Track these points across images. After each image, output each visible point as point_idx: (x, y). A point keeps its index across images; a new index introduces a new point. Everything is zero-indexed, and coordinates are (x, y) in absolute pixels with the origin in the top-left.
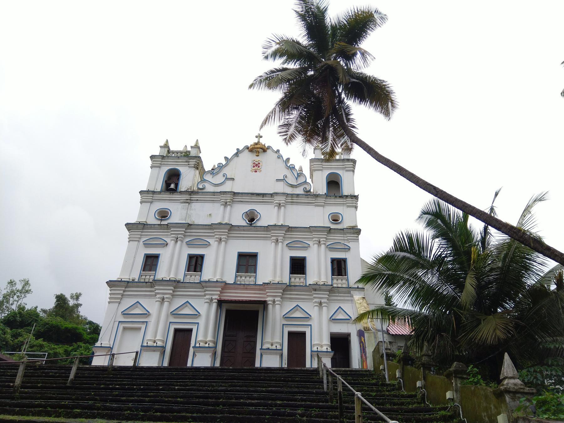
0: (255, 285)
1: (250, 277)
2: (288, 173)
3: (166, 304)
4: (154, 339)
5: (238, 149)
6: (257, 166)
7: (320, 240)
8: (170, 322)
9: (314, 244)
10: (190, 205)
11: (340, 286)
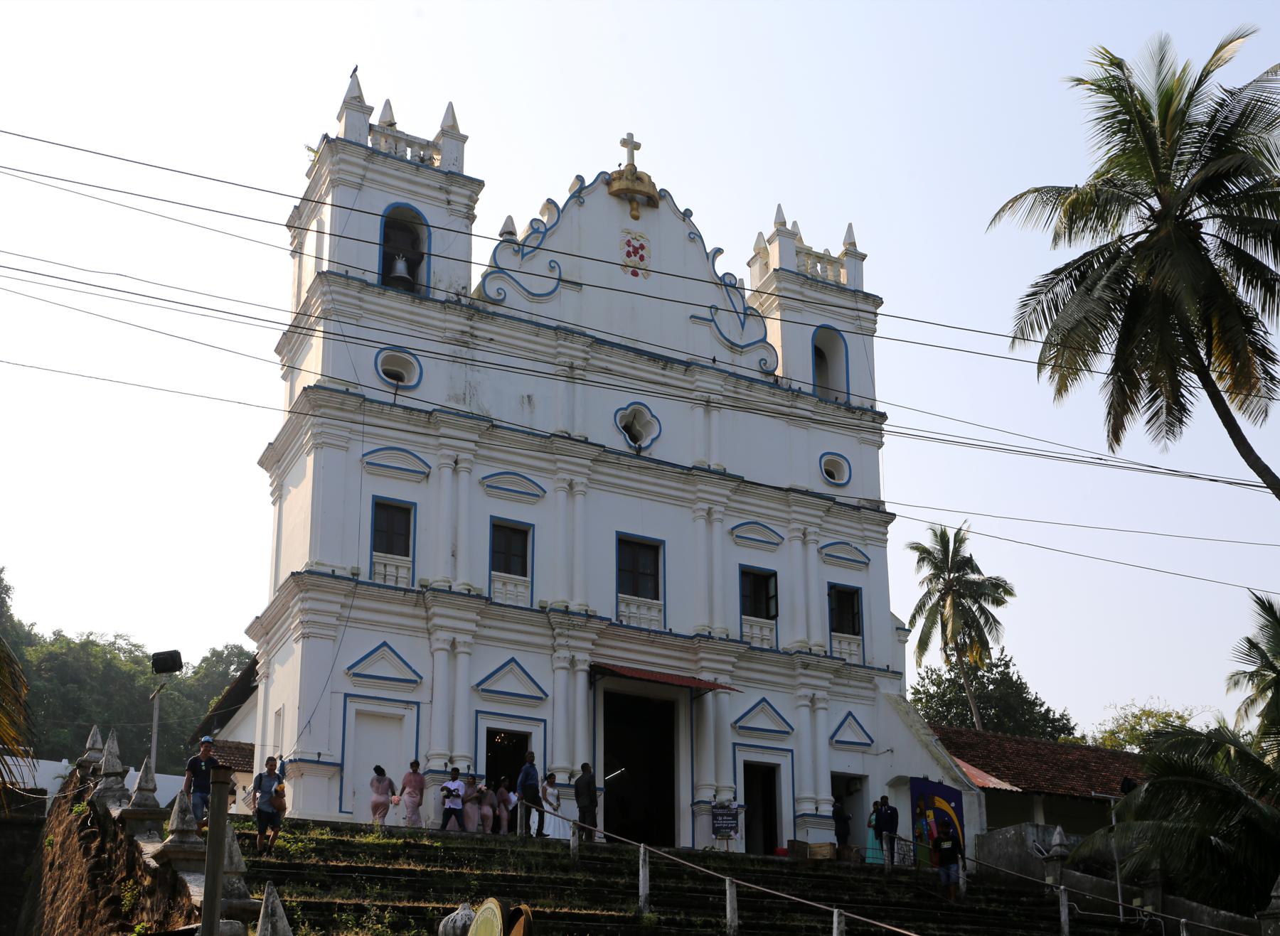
1: (649, 608)
2: (716, 296)
3: (462, 660)
4: (448, 753)
6: (638, 256)
7: (805, 529)
9: (790, 539)
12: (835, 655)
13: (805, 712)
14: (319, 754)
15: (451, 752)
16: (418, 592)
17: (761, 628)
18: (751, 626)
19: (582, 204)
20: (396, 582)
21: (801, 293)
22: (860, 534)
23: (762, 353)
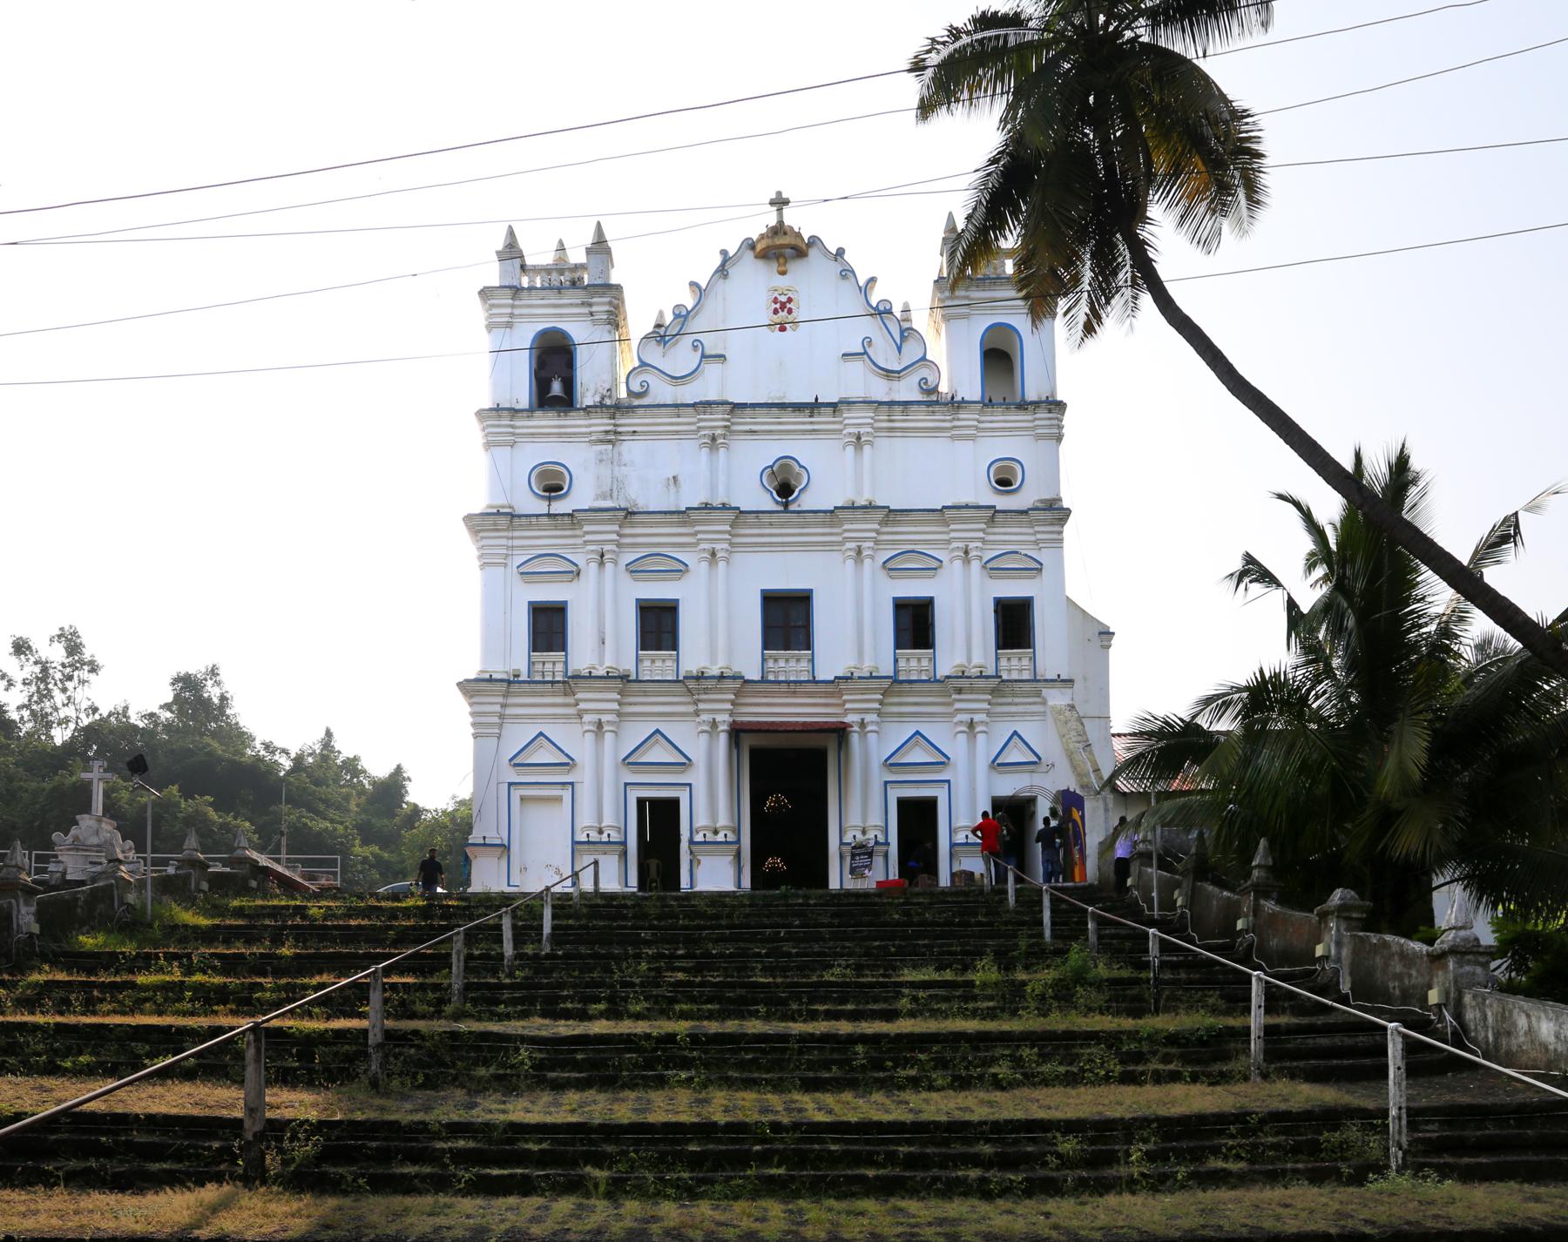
0: (814, 681)
1: (798, 660)
2: (870, 327)
3: (609, 737)
4: (597, 825)
5: (724, 253)
6: (786, 310)
7: (967, 546)
8: (626, 784)
9: (951, 561)
10: (616, 449)
11: (1015, 676)
13: (962, 738)
15: (600, 824)
16: (564, 682)
17: (919, 660)
18: (908, 660)
19: (725, 276)
20: (554, 676)
22: (1033, 538)
23: (924, 373)
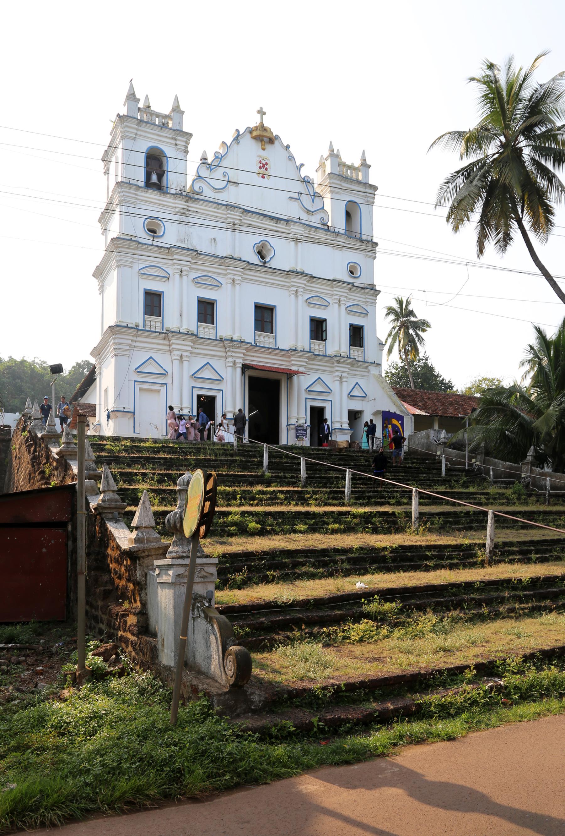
1: (269, 338)
2: (300, 187)
3: (186, 363)
9: (333, 304)
12: (352, 357)
13: (337, 383)
14: (124, 408)
15: (181, 404)
16: (165, 333)
17: (319, 345)
19: (238, 143)
21: (340, 185)
23: (322, 215)
